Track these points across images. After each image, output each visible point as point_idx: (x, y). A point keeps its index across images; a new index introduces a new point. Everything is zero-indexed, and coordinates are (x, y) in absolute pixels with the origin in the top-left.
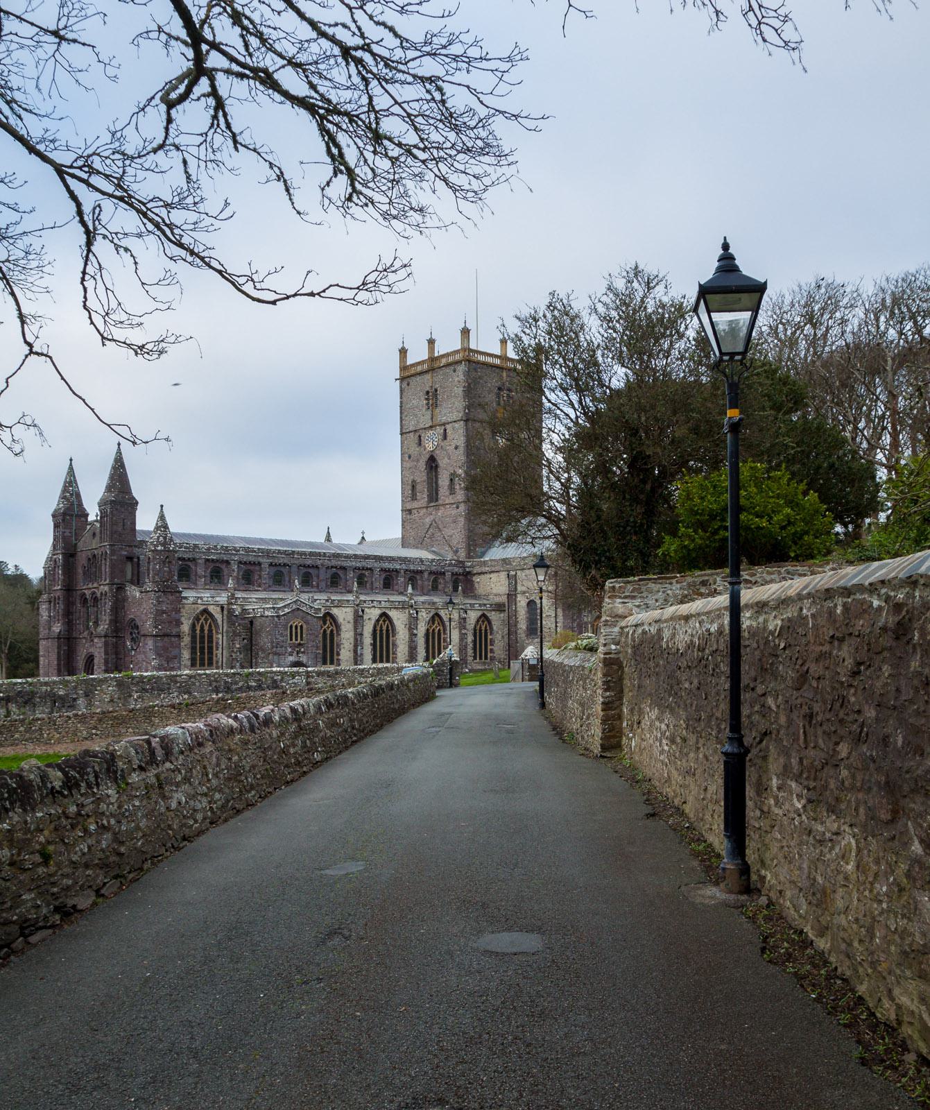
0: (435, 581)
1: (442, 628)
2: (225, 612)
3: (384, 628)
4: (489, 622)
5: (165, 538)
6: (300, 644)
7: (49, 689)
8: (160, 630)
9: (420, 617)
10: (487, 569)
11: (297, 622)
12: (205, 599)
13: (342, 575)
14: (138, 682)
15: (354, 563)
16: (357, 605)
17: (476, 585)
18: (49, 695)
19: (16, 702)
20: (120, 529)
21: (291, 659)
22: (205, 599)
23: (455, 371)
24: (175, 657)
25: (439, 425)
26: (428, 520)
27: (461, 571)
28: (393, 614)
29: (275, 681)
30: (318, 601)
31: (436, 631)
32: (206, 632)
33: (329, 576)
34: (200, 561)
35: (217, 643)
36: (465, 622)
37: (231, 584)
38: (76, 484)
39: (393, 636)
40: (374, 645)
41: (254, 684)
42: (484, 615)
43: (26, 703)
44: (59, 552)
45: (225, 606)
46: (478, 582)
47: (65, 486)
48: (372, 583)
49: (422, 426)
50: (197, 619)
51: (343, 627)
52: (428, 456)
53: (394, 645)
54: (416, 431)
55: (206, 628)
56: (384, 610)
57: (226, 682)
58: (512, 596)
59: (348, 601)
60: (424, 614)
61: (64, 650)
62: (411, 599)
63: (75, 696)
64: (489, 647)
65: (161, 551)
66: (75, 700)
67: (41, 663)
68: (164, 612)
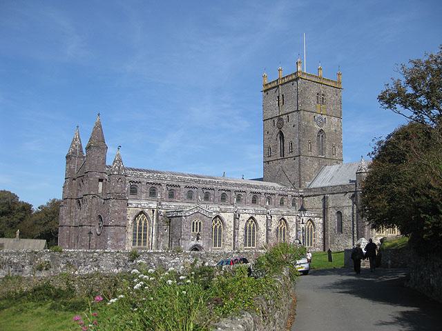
0: (282, 200)
3: (252, 226)
5: (119, 167)
7: (8, 257)
9: (273, 220)
21: (193, 243)
26: (277, 167)
27: (297, 194)
28: (257, 217)
32: (143, 225)
50: (137, 216)
52: (278, 131)
55: (143, 222)
57: (124, 260)
63: (23, 264)
66: (23, 266)
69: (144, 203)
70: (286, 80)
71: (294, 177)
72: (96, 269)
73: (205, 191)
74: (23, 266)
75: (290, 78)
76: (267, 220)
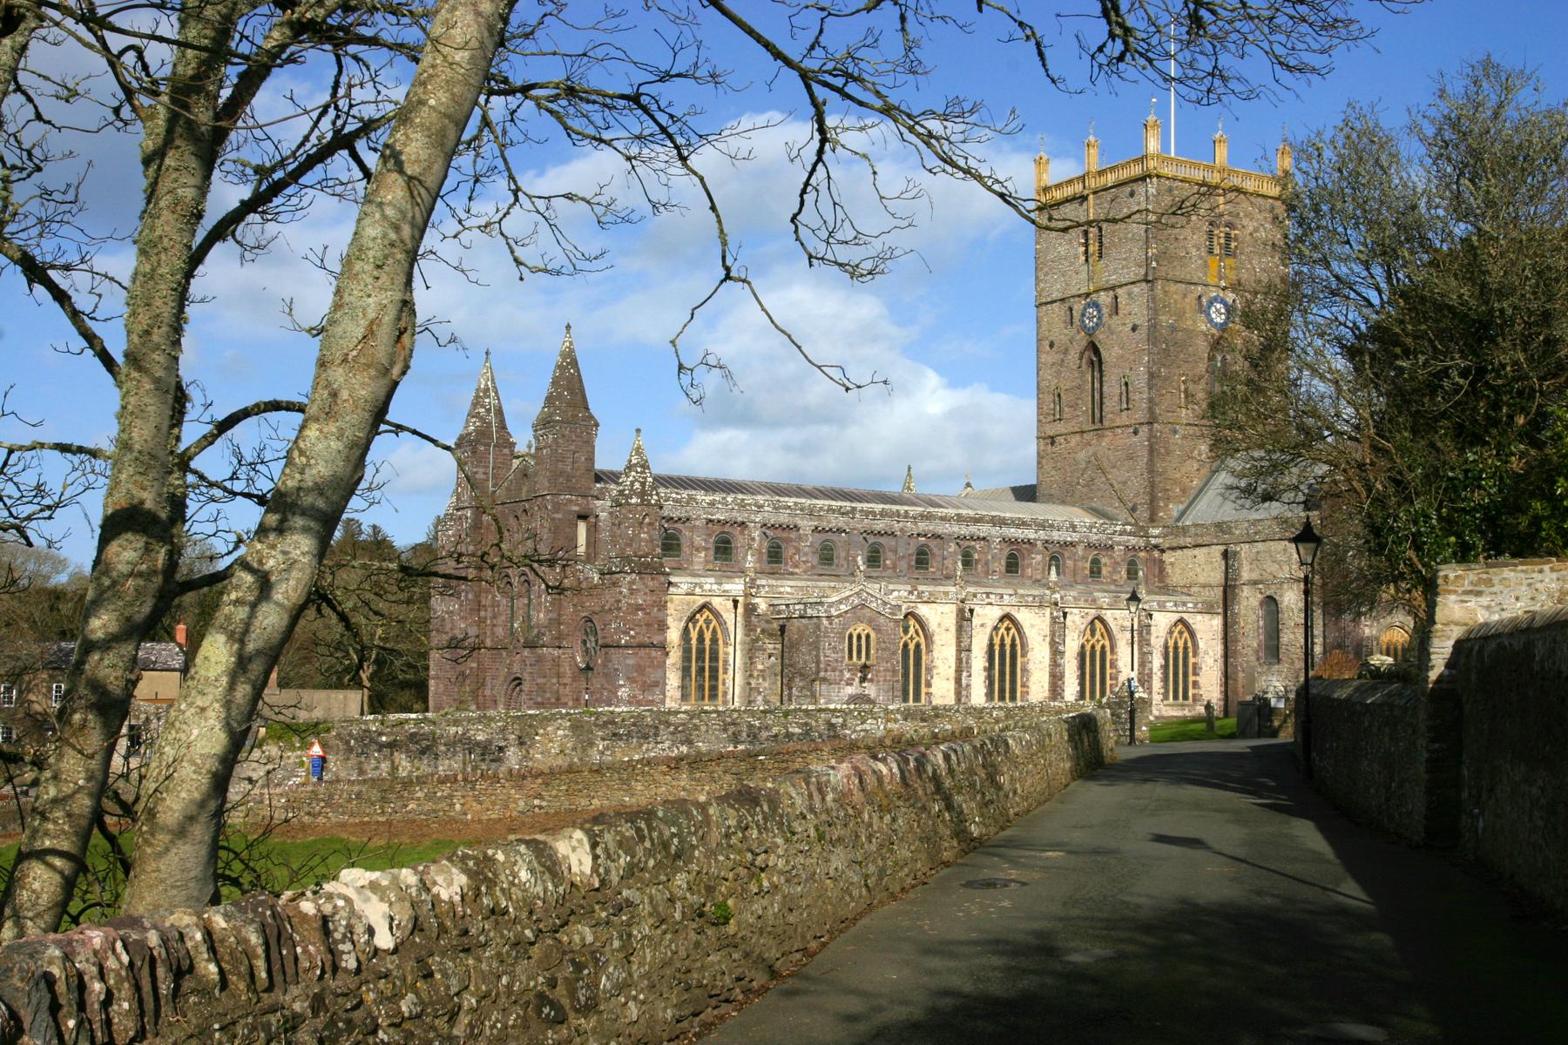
0: (1096, 562)
1: (1107, 644)
2: (740, 609)
3: (1008, 641)
4: (1192, 634)
5: (643, 484)
6: (865, 668)
8: (631, 637)
10: (1189, 540)
11: (861, 629)
12: (707, 587)
13: (935, 550)
14: (606, 724)
15: (956, 529)
16: (962, 602)
17: (1169, 570)
18: (460, 741)
19: (408, 751)
20: (569, 469)
21: (850, 690)
22: (707, 587)
23: (1132, 194)
24: (656, 684)
25: (1105, 290)
26: (1082, 455)
27: (1142, 542)
28: (1023, 616)
29: (831, 726)
30: (896, 594)
31: (1098, 648)
32: (707, 642)
33: (912, 550)
34: (698, 523)
35: (726, 662)
36: (1149, 633)
37: (750, 562)
38: (496, 393)
39: (1022, 656)
40: (990, 669)
41: (797, 730)
42: (1181, 621)
43: (423, 752)
44: (466, 504)
45: (741, 599)
46: (1172, 564)
47: (477, 397)
48: (987, 564)
49: (1074, 292)
50: (692, 619)
51: (936, 638)
52: (1084, 343)
53: (1024, 670)
54: (1062, 300)
55: (708, 636)
56: (1007, 610)
57: (750, 726)
58: (1229, 591)
59: (946, 594)
60: (1077, 619)
61: (471, 668)
62: (1054, 592)
63: (502, 744)
64: (1191, 678)
65: (637, 505)
67: (432, 689)
68: (638, 608)
69: (709, 583)
70: (1111, 179)
71: (1135, 486)
72: (684, 749)
73: (871, 539)
74: (501, 749)
75: (1124, 174)
76: (1054, 620)
